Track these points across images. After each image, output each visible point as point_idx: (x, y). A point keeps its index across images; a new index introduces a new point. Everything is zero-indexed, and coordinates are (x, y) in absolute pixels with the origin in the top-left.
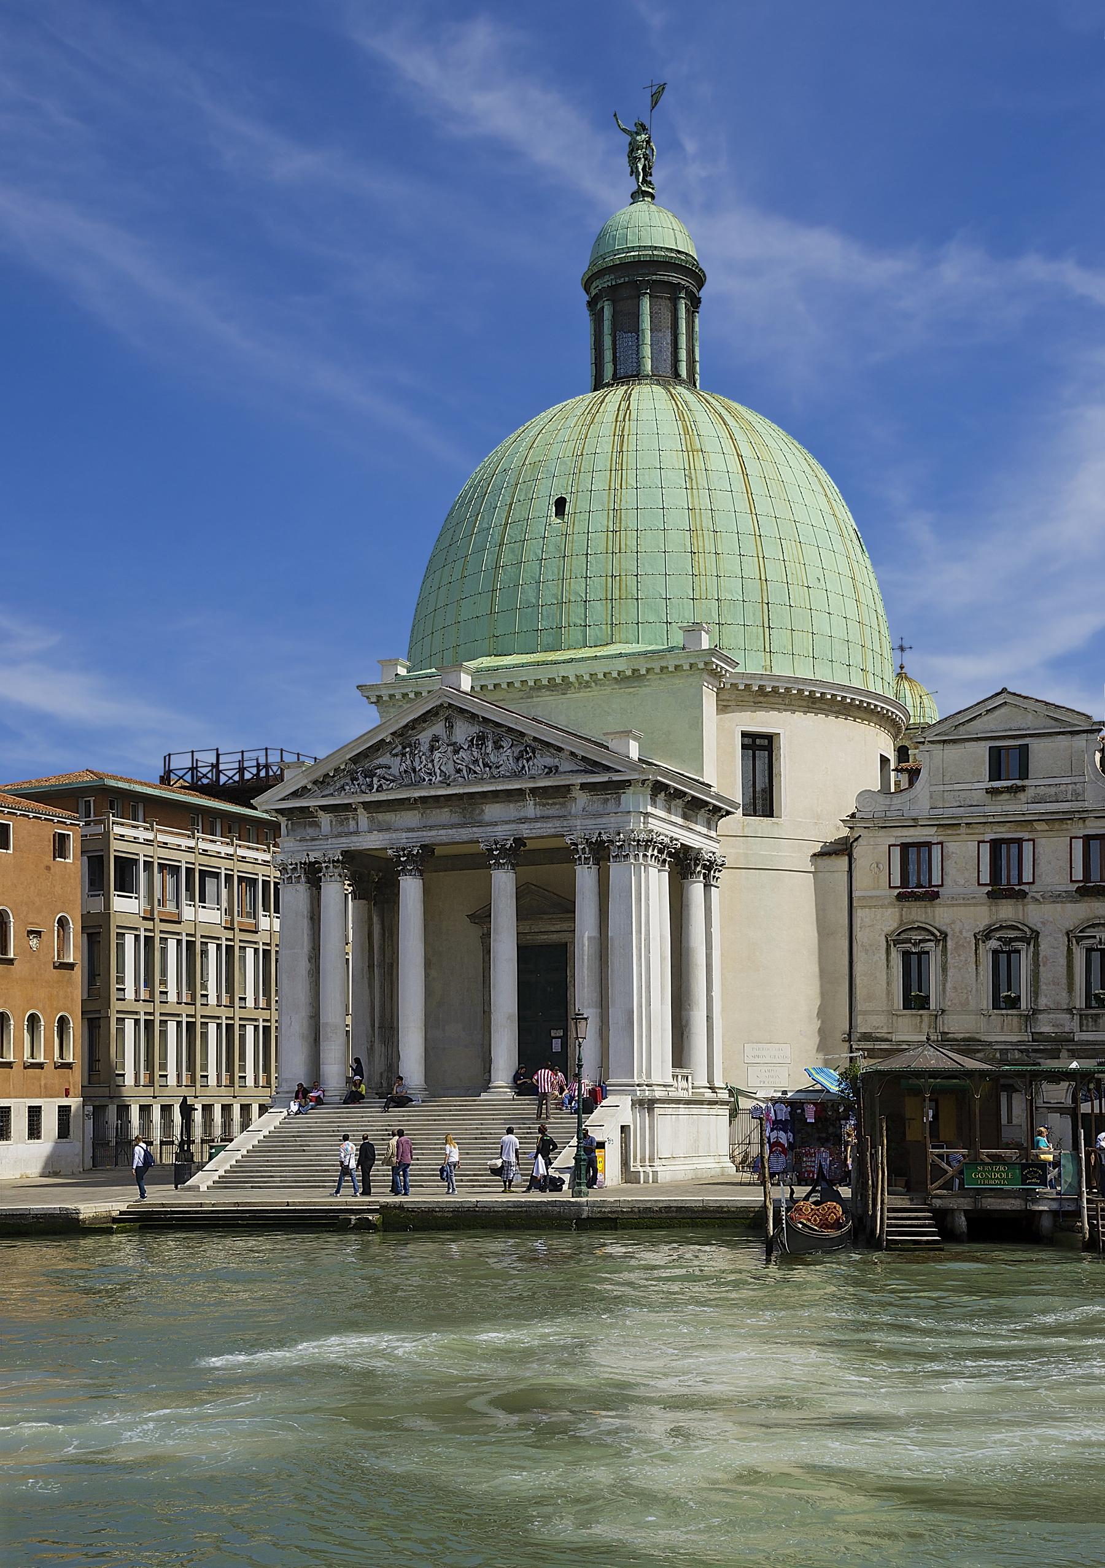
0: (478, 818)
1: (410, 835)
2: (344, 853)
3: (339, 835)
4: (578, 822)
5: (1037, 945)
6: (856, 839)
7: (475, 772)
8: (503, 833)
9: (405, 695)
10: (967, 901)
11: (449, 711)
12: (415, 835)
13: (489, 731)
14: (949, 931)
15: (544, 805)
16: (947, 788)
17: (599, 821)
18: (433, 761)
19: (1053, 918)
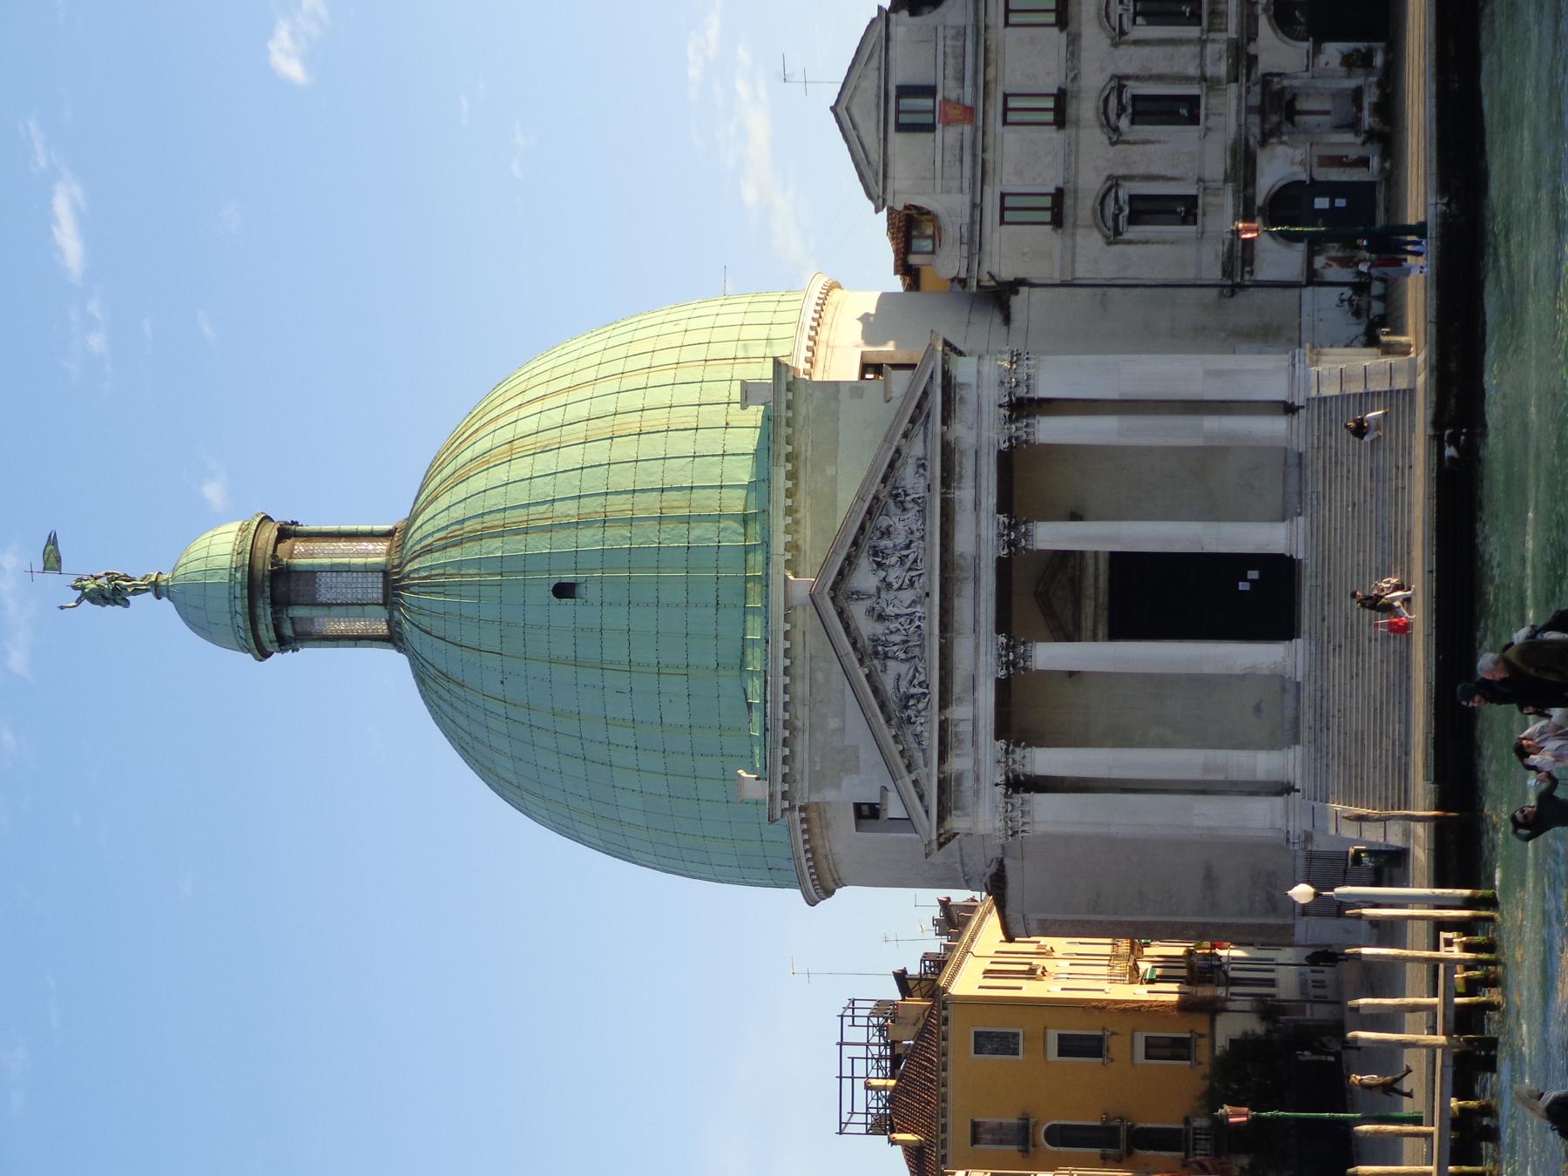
0: (970, 561)
1: (982, 650)
2: (997, 739)
3: (975, 743)
4: (985, 434)
5: (1128, 77)
6: (992, 277)
7: (915, 561)
9: (785, 760)
10: (1072, 150)
11: (839, 588)
12: (983, 643)
13: (866, 545)
14: (1106, 173)
15: (961, 477)
16: (938, 174)
17: (985, 409)
18: (897, 616)
19: (1100, 62)
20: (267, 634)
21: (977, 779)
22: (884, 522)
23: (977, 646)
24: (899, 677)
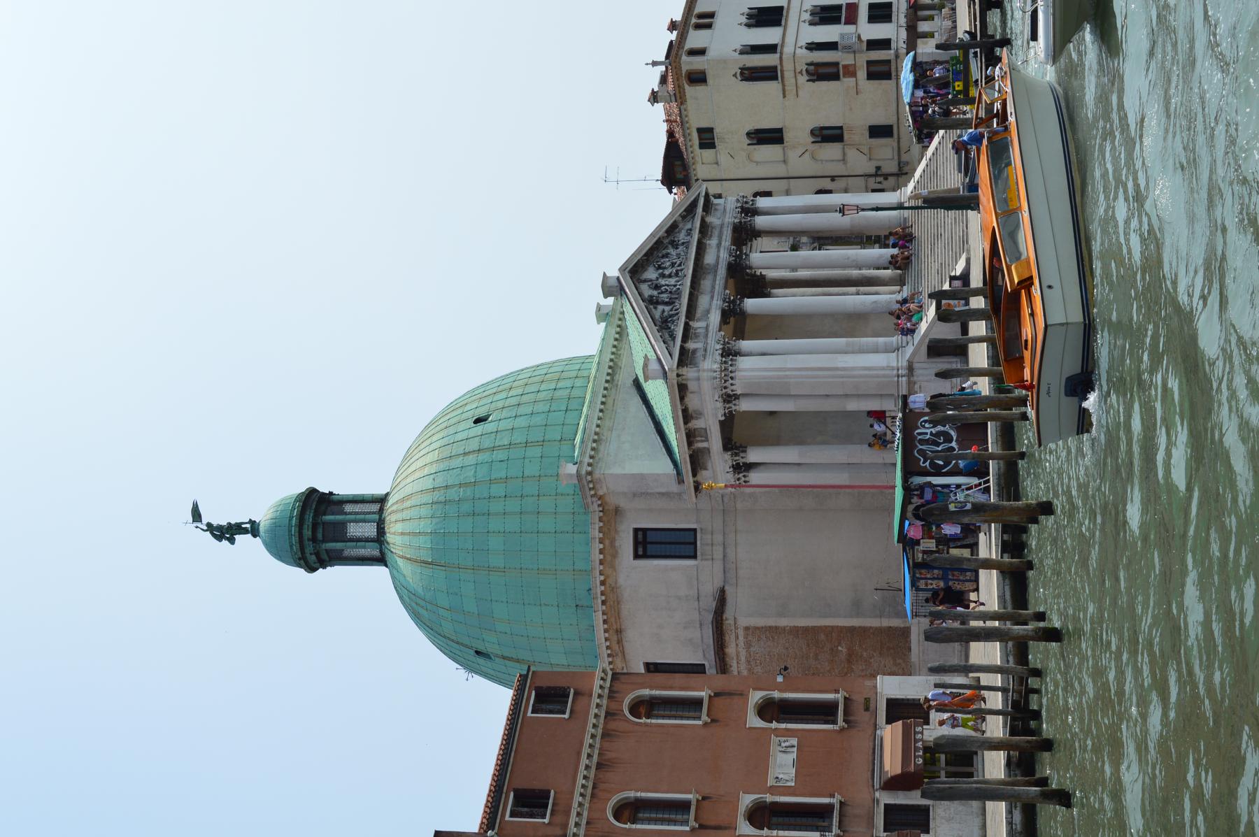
8: (724, 255)
20: (308, 533)
21: (705, 350)
23: (712, 297)
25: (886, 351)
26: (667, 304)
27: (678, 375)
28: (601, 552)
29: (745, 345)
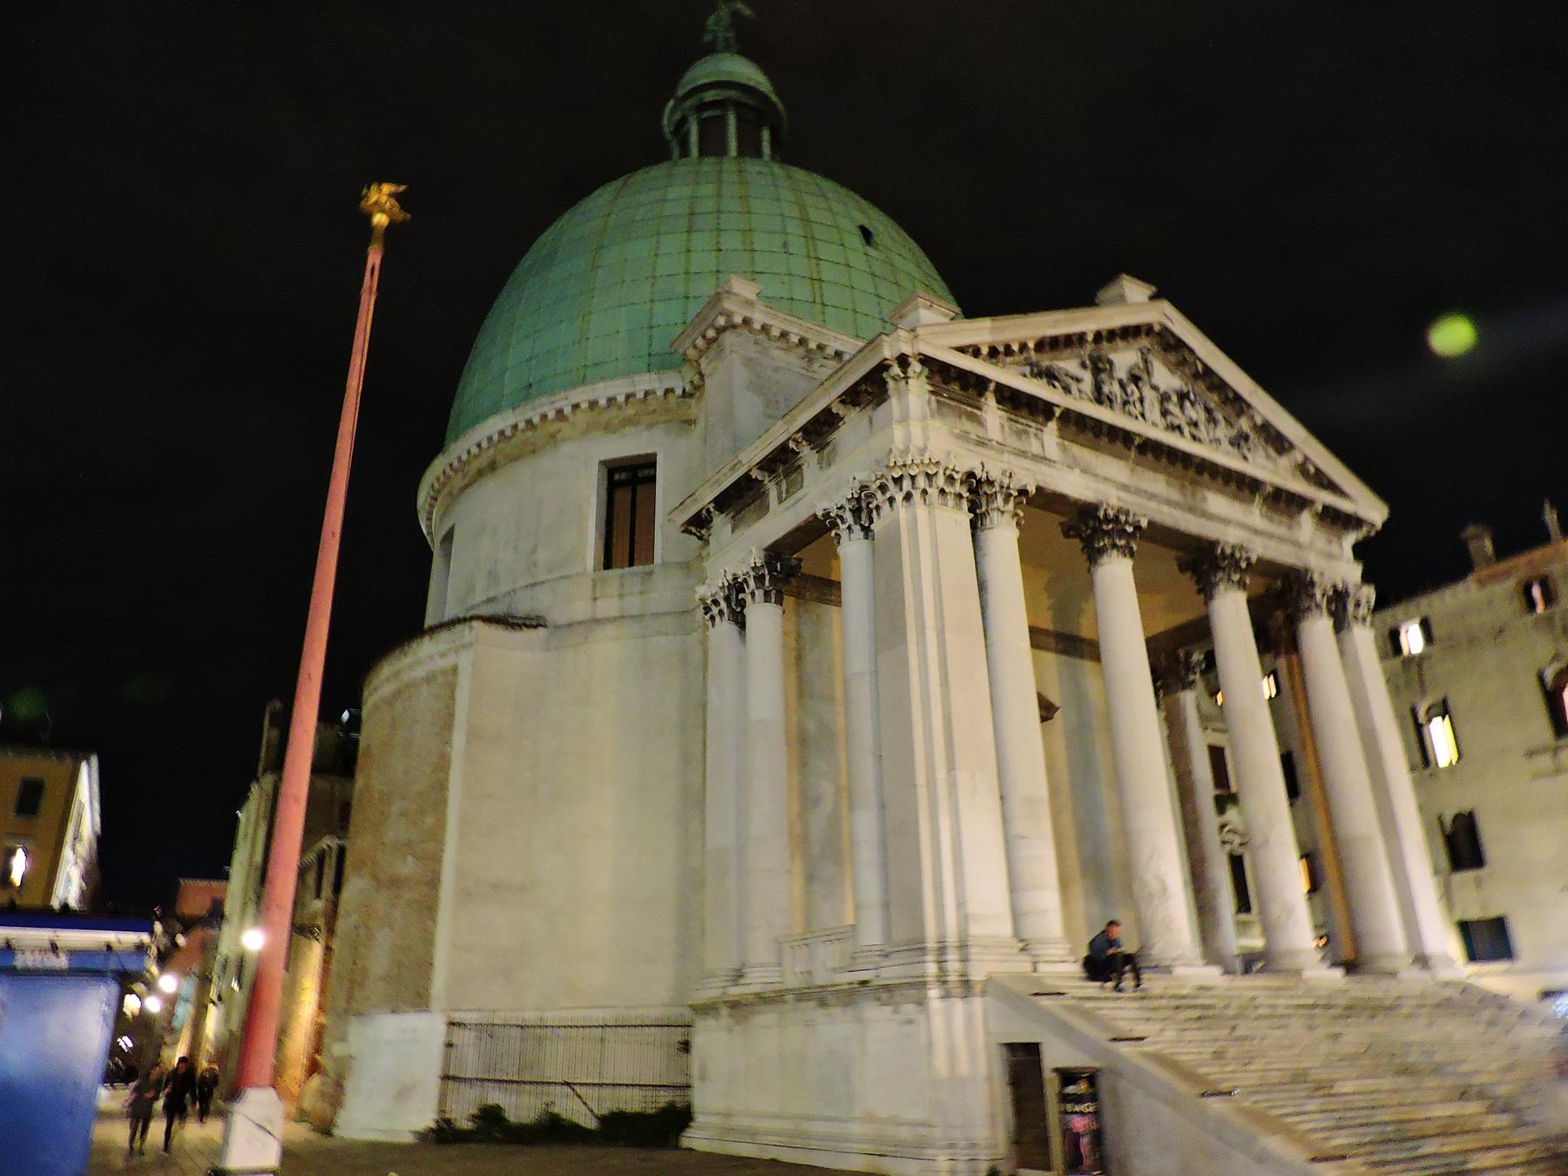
18: (1141, 400)
20: (710, 96)
22: (1219, 416)
24: (1078, 380)
25: (1016, 915)
26: (1098, 388)
27: (903, 360)
28: (611, 400)
29: (1004, 535)
